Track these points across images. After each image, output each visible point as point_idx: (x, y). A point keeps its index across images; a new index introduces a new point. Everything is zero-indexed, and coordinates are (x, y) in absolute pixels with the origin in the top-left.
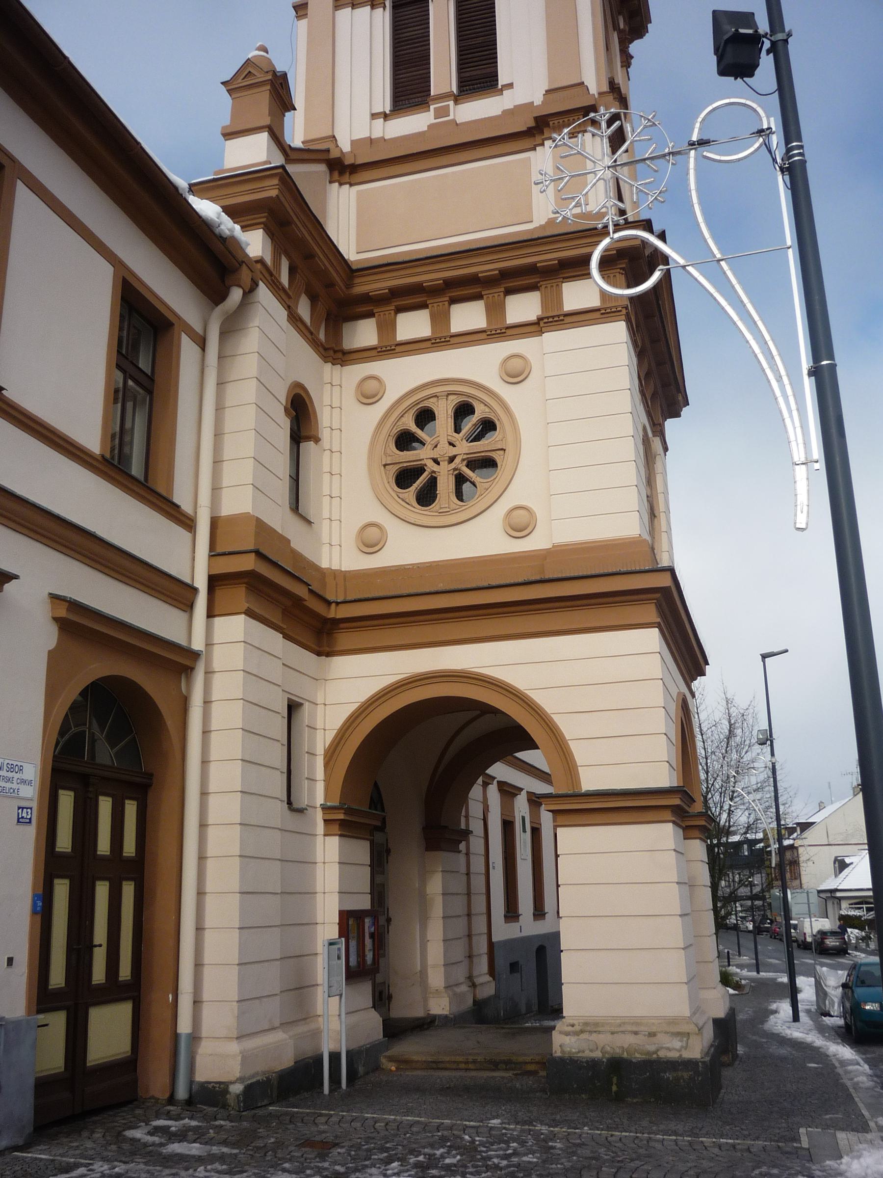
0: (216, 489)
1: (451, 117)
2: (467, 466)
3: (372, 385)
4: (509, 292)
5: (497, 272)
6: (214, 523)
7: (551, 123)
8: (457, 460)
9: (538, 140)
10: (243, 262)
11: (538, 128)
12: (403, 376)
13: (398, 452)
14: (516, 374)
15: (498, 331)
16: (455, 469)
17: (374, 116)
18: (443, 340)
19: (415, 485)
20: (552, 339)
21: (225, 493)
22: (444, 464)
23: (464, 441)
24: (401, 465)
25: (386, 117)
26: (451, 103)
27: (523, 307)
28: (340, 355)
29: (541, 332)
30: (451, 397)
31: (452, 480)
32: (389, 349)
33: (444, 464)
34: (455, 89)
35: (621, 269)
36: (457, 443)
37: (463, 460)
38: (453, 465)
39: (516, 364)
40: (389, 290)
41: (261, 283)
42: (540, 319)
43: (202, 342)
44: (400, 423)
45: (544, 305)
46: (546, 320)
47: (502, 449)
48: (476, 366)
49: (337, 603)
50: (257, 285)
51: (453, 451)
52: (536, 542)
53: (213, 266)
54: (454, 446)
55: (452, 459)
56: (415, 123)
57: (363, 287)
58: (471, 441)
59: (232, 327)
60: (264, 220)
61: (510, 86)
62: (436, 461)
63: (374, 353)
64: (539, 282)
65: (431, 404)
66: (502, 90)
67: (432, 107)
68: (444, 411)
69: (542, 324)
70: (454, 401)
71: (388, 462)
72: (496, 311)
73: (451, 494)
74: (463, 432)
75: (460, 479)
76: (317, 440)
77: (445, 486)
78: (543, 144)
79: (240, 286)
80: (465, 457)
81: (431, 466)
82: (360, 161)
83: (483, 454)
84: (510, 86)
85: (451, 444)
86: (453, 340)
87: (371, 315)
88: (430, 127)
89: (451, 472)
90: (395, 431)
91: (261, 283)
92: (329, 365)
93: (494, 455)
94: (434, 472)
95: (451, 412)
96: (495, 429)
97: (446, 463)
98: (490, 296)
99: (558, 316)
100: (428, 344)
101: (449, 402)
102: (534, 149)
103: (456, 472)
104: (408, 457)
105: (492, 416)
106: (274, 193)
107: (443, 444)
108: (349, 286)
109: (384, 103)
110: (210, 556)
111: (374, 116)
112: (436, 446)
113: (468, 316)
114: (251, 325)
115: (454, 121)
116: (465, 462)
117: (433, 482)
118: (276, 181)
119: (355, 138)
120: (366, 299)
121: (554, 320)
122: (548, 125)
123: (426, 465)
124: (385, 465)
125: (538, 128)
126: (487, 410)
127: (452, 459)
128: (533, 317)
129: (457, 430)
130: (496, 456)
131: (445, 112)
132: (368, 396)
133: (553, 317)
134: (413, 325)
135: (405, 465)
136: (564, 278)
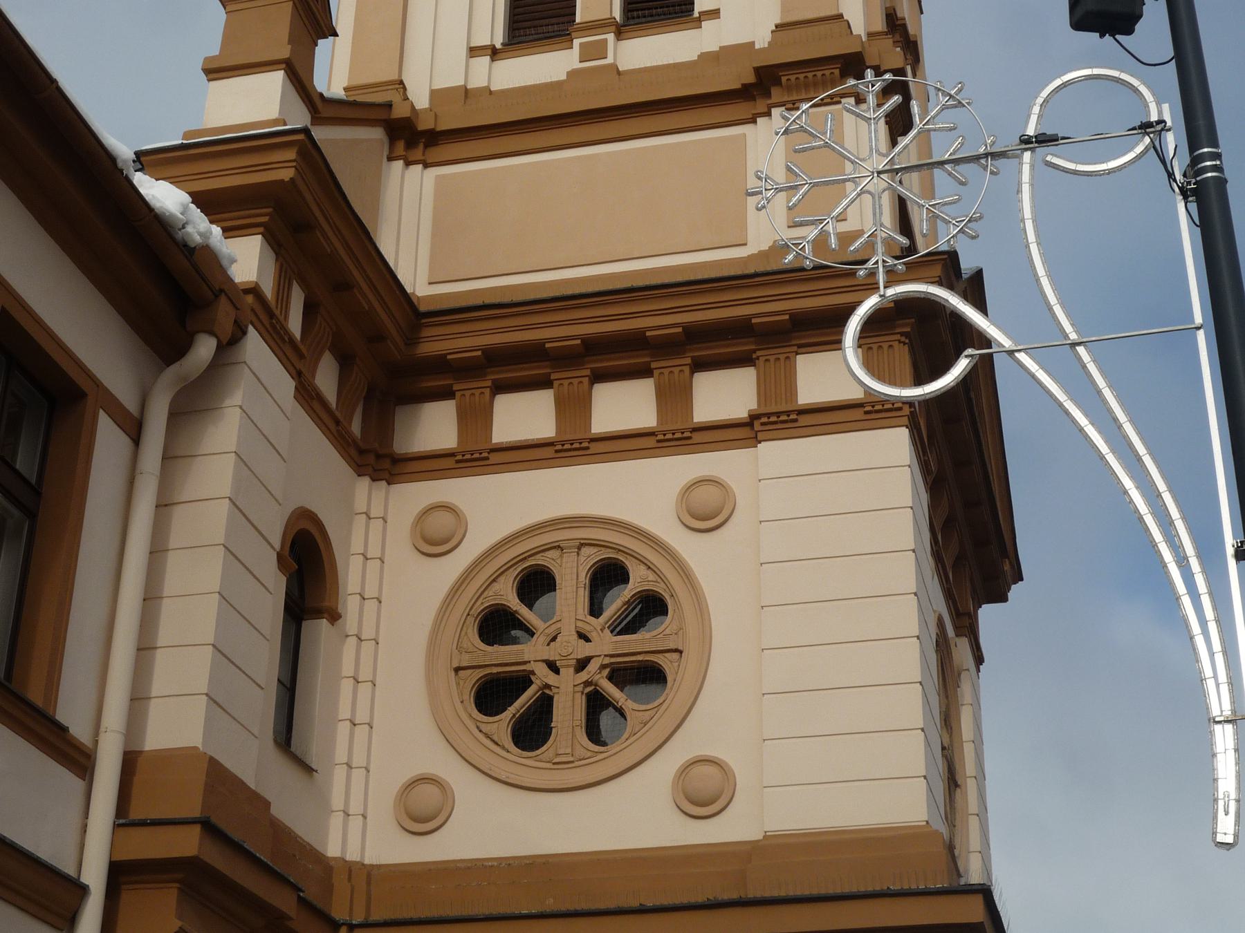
0: (138, 700)
1: (609, 60)
2: (610, 678)
3: (441, 522)
4: (701, 365)
5: (680, 330)
6: (130, 762)
7: (784, 79)
8: (593, 666)
9: (761, 105)
10: (222, 291)
11: (762, 85)
12: (500, 508)
13: (483, 646)
14: (706, 512)
15: (677, 435)
16: (587, 683)
17: (474, 51)
18: (574, 446)
19: (511, 710)
20: (776, 454)
21: (156, 710)
22: (567, 673)
23: (607, 631)
24: (488, 671)
25: (494, 53)
26: (611, 37)
27: (724, 394)
28: (386, 464)
29: (755, 441)
30: (586, 551)
31: (581, 702)
32: (478, 457)
33: (567, 673)
34: (617, 14)
35: (902, 334)
36: (593, 636)
37: (603, 667)
38: (584, 676)
39: (707, 496)
40: (484, 351)
41: (251, 328)
42: (753, 417)
43: (134, 429)
44: (490, 592)
45: (763, 391)
46: (764, 420)
47: (676, 651)
48: (637, 496)
49: (352, 927)
50: (244, 333)
51: (584, 650)
53: (166, 295)
54: (587, 640)
55: (582, 664)
56: (546, 67)
57: (435, 344)
58: (620, 633)
59: (192, 406)
60: (265, 219)
61: (714, 14)
62: (553, 667)
63: (450, 463)
64: (754, 351)
65: (548, 560)
66: (699, 20)
67: (576, 42)
68: (572, 578)
69: (757, 426)
70: (591, 557)
71: (465, 664)
72: (674, 398)
73: (578, 730)
74: (607, 614)
75: (596, 703)
76: (334, 617)
77: (568, 712)
78: (768, 114)
79: (212, 333)
80: (607, 661)
81: (542, 674)
82: (443, 126)
83: (640, 658)
84: (714, 14)
85: (583, 637)
86: (595, 448)
87: (445, 394)
88: (572, 74)
89: (580, 688)
90: (479, 607)
91: (251, 328)
92: (365, 482)
93: (659, 659)
94: (548, 686)
95: (584, 579)
96: (666, 614)
97: (572, 670)
98: (666, 371)
99: (788, 413)
100: (549, 452)
101: (582, 559)
102: (753, 121)
103: (591, 688)
104: (501, 655)
105: (660, 588)
106: (287, 174)
107: (567, 634)
108: (412, 339)
109: (492, 29)
110: (117, 826)
111: (474, 51)
112: (554, 639)
113: (624, 405)
114: (228, 402)
115: (614, 67)
116: (606, 672)
117: (545, 704)
118: (291, 154)
119: (440, 84)
120: (441, 365)
121: (778, 419)
123: (533, 673)
124: (457, 670)
125: (762, 85)
126: (652, 577)
127: (582, 664)
128: (741, 413)
129: (595, 610)
130: (664, 661)
131: (598, 51)
132: (434, 541)
133: (778, 414)
134: (524, 416)
135: (495, 670)
136: (800, 346)
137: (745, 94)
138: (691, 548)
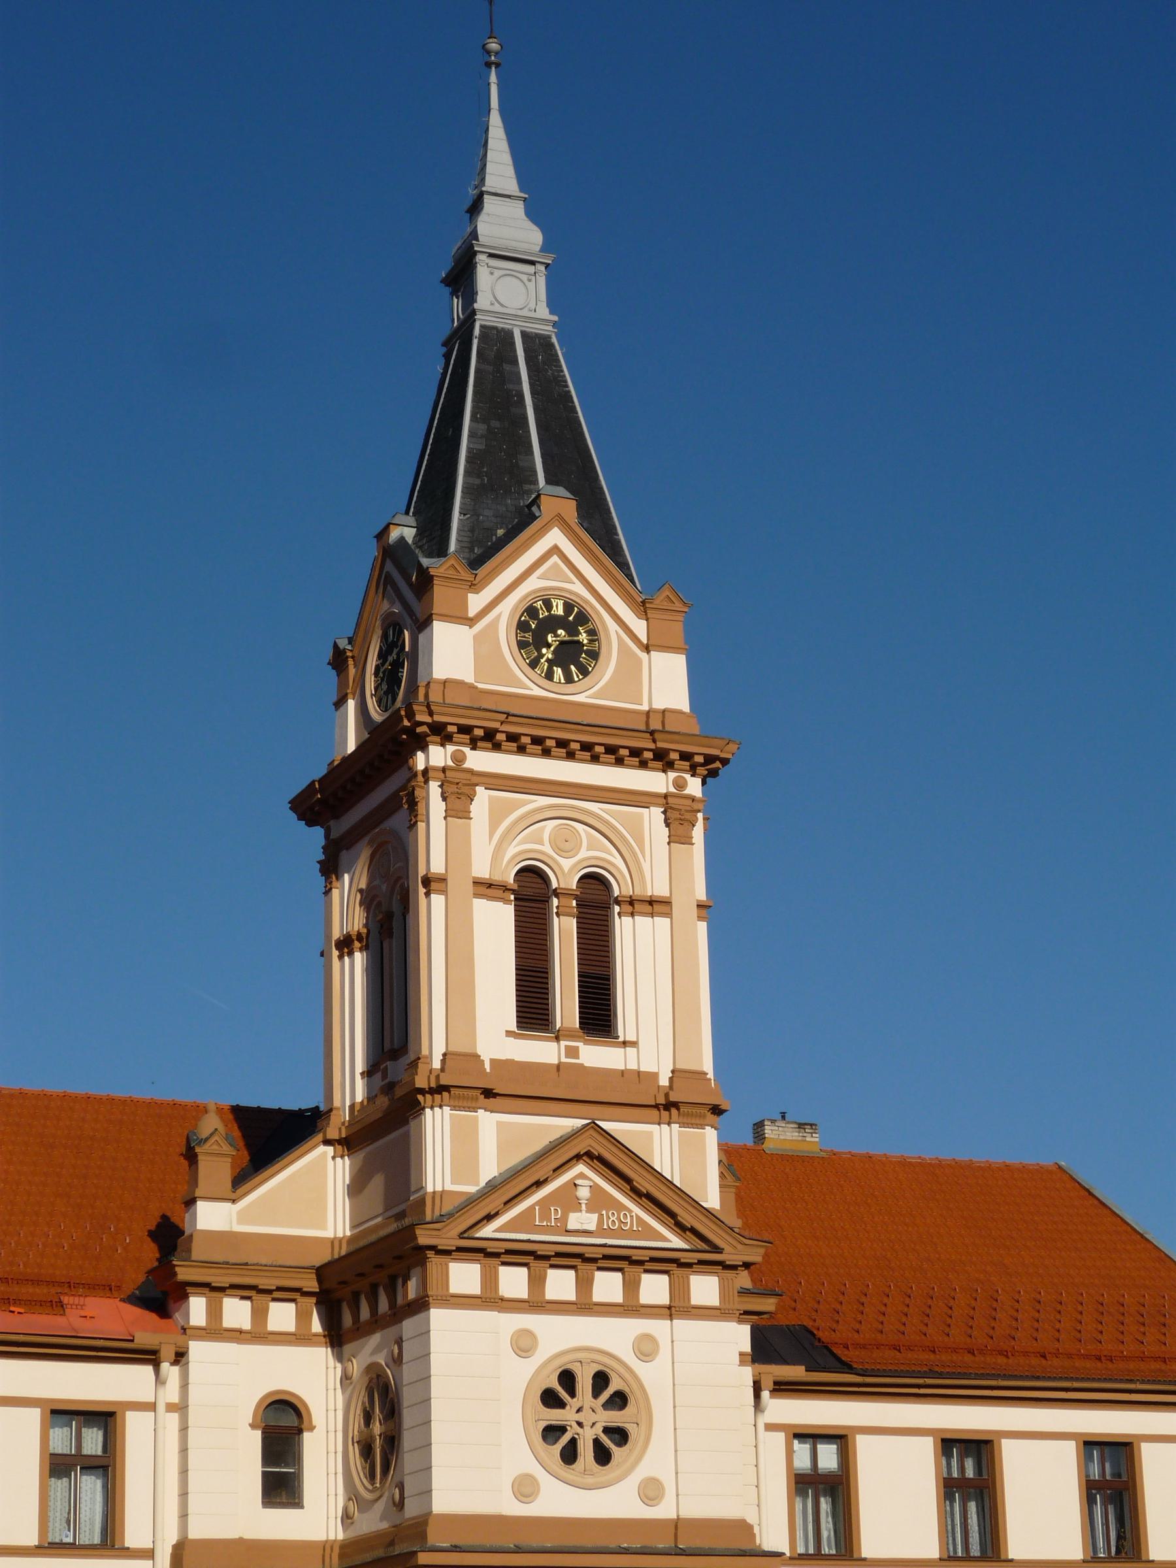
9: (665, 1114)
15: (630, 1308)
27: (655, 1288)
52: (665, 1511)
56: (541, 1051)
61: (634, 1044)
67: (563, 1043)
70: (596, 1368)
84: (634, 1044)
104: (555, 1416)
105: (626, 1390)
113: (608, 1286)
121: (678, 1308)
122: (678, 1109)
125: (667, 1107)
131: (573, 1052)
137: (656, 1106)
138: (643, 1370)
